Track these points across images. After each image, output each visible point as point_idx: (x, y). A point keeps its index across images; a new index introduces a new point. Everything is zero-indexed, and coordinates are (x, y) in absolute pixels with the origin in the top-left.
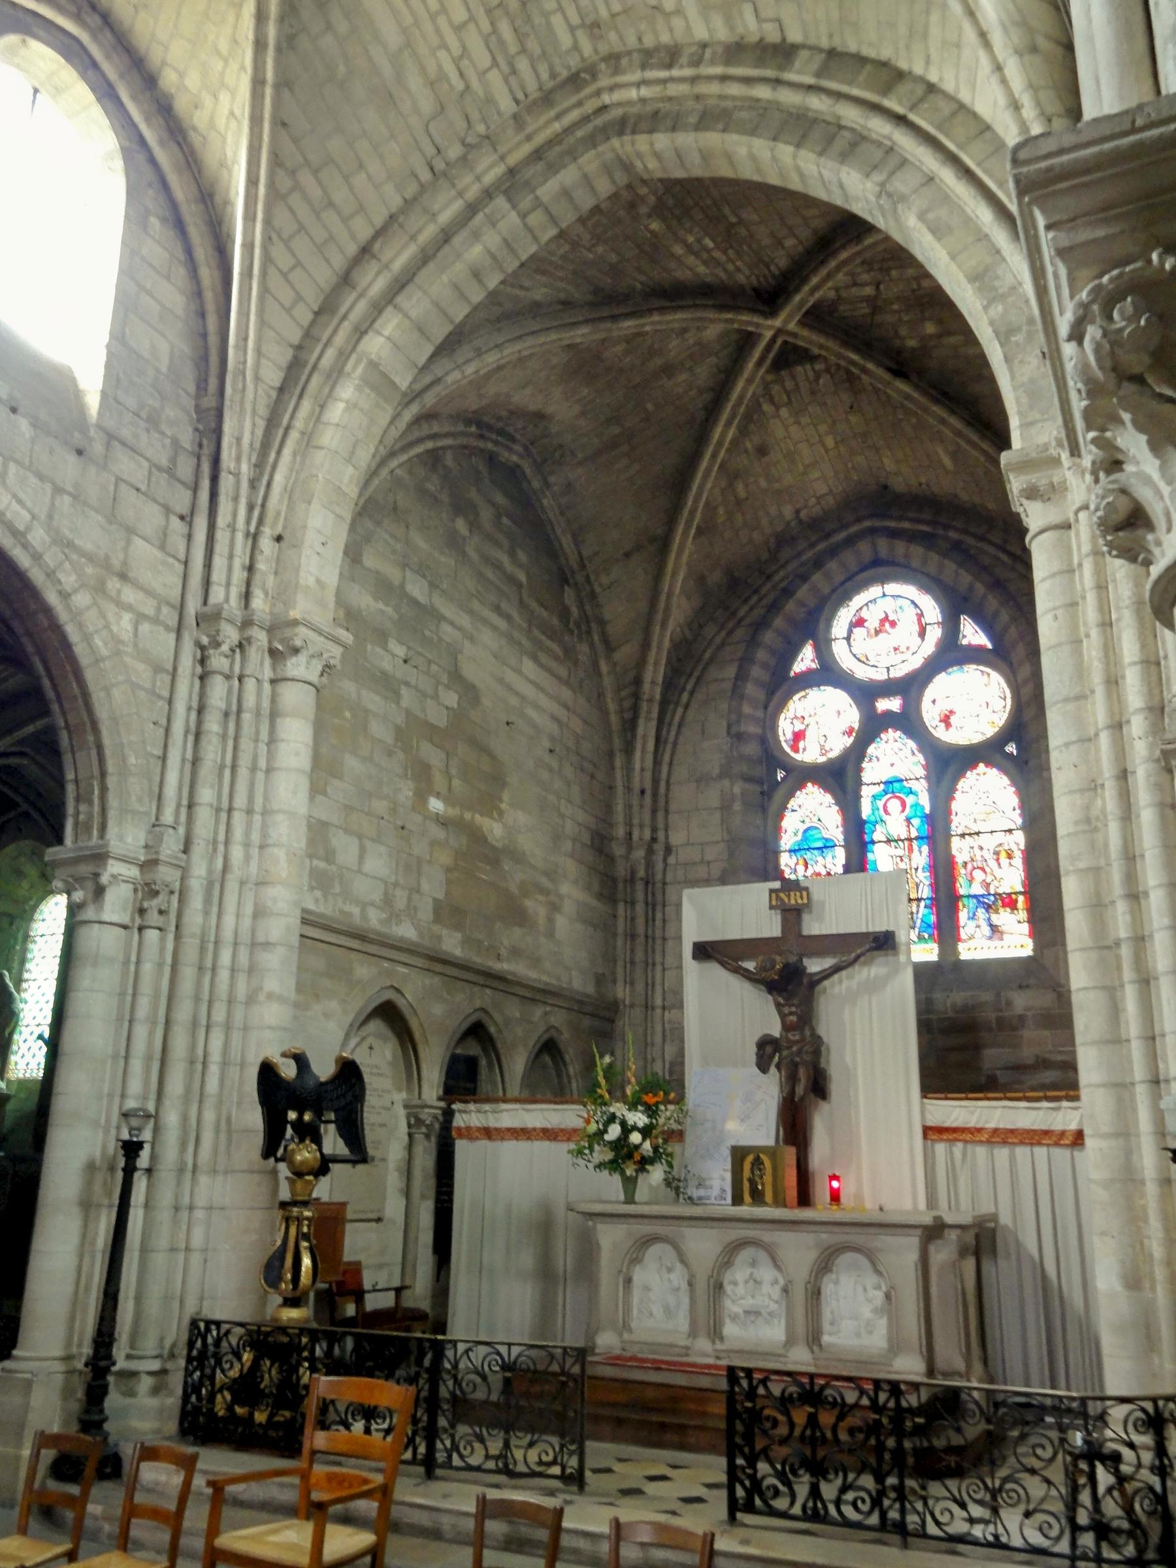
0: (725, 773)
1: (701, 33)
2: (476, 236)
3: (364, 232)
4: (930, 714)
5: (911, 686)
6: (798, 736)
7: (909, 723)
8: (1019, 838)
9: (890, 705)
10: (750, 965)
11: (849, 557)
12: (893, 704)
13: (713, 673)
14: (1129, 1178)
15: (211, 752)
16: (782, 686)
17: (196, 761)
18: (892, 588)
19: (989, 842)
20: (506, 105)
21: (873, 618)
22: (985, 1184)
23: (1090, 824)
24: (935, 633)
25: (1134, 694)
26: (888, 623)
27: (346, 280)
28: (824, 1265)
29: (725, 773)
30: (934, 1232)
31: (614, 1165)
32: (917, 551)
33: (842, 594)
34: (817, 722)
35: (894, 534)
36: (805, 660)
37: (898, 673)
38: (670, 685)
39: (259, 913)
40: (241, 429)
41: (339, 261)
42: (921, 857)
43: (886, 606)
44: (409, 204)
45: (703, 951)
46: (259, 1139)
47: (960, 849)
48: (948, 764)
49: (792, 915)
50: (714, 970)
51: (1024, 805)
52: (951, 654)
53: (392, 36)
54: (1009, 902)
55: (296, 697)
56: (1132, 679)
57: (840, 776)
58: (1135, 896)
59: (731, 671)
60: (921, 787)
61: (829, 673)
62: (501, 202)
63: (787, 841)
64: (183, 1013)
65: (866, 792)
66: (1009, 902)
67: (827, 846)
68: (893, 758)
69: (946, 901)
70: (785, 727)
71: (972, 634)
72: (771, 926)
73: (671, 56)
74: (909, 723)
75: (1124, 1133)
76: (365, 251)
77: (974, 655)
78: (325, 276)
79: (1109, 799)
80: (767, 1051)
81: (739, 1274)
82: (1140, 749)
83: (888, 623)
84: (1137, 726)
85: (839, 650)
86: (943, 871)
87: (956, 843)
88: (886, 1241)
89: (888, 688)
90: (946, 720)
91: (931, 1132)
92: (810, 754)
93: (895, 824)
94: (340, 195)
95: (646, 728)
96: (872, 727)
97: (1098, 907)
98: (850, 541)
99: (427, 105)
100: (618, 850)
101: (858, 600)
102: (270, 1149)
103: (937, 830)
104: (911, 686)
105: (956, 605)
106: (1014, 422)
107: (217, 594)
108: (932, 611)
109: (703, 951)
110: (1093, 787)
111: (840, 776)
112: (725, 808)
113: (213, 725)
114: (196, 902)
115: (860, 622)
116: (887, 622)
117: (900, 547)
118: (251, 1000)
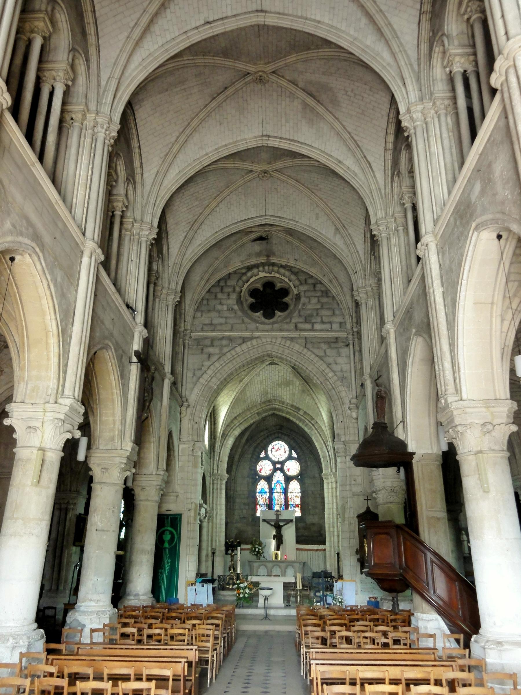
0: (248, 477)
1: (288, 401)
2: (252, 419)
3: (236, 415)
4: (286, 468)
5: (282, 463)
6: (261, 470)
7: (282, 470)
8: (300, 495)
9: (278, 466)
10: (273, 524)
11: (273, 436)
12: (278, 466)
13: (246, 456)
14: (331, 556)
15: (215, 496)
16: (258, 459)
17: (213, 497)
18: (280, 442)
19: (295, 494)
20: (259, 402)
21: (276, 447)
22: (304, 556)
23: (329, 518)
24: (287, 453)
25: (335, 507)
26: (279, 450)
27: (232, 421)
28: (286, 568)
29: (248, 477)
30: (300, 563)
31: (257, 555)
32: (286, 438)
33: (271, 442)
34: (264, 467)
35: (282, 434)
36: (263, 455)
37: (281, 460)
38: (240, 458)
39: (221, 519)
40: (218, 445)
41: (231, 419)
42: (283, 496)
43: (279, 446)
44: (243, 412)
45: (264, 520)
46: (224, 552)
47: (290, 495)
48: (288, 479)
49: (278, 516)
50: (265, 523)
51: (301, 488)
52: (290, 458)
53: (248, 395)
54: (297, 506)
55: (224, 487)
56: (335, 504)
57: (269, 479)
58: (333, 527)
59: (250, 456)
60: (283, 483)
61: (267, 458)
62: (256, 415)
63: (258, 491)
64: (214, 534)
65: (273, 483)
66: (297, 506)
67: (266, 492)
68: (278, 476)
69: (287, 505)
70: (258, 467)
71: (294, 455)
72: (274, 517)
73: (283, 403)
74: (282, 470)
75: (330, 551)
76: (235, 418)
77: (293, 458)
78: (229, 421)
79: (331, 516)
80: (274, 537)
81: (274, 569)
82: (335, 512)
83: (279, 450)
84: (335, 509)
85: (269, 453)
86: (286, 499)
87: (289, 494)
88: (295, 564)
89: (278, 462)
90: (288, 470)
91: (297, 549)
92: (263, 473)
93: (279, 490)
94: (235, 411)
95: (234, 467)
96: (275, 470)
97: (329, 528)
98: (274, 433)
99: (249, 402)
100: (229, 492)
101: (274, 443)
102: (226, 553)
103: (286, 491)
104: (282, 463)
105: (291, 448)
106: (324, 469)
107: (215, 471)
108: (287, 449)
109: (264, 520)
110: (329, 514)
111: (269, 479)
112: (248, 484)
113: (215, 491)
114: (215, 519)
115: (273, 448)
116: (279, 449)
117: (283, 436)
118: (220, 532)
